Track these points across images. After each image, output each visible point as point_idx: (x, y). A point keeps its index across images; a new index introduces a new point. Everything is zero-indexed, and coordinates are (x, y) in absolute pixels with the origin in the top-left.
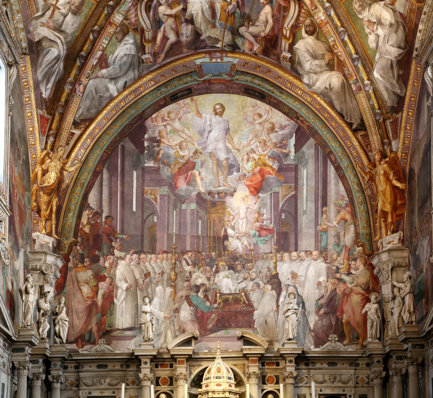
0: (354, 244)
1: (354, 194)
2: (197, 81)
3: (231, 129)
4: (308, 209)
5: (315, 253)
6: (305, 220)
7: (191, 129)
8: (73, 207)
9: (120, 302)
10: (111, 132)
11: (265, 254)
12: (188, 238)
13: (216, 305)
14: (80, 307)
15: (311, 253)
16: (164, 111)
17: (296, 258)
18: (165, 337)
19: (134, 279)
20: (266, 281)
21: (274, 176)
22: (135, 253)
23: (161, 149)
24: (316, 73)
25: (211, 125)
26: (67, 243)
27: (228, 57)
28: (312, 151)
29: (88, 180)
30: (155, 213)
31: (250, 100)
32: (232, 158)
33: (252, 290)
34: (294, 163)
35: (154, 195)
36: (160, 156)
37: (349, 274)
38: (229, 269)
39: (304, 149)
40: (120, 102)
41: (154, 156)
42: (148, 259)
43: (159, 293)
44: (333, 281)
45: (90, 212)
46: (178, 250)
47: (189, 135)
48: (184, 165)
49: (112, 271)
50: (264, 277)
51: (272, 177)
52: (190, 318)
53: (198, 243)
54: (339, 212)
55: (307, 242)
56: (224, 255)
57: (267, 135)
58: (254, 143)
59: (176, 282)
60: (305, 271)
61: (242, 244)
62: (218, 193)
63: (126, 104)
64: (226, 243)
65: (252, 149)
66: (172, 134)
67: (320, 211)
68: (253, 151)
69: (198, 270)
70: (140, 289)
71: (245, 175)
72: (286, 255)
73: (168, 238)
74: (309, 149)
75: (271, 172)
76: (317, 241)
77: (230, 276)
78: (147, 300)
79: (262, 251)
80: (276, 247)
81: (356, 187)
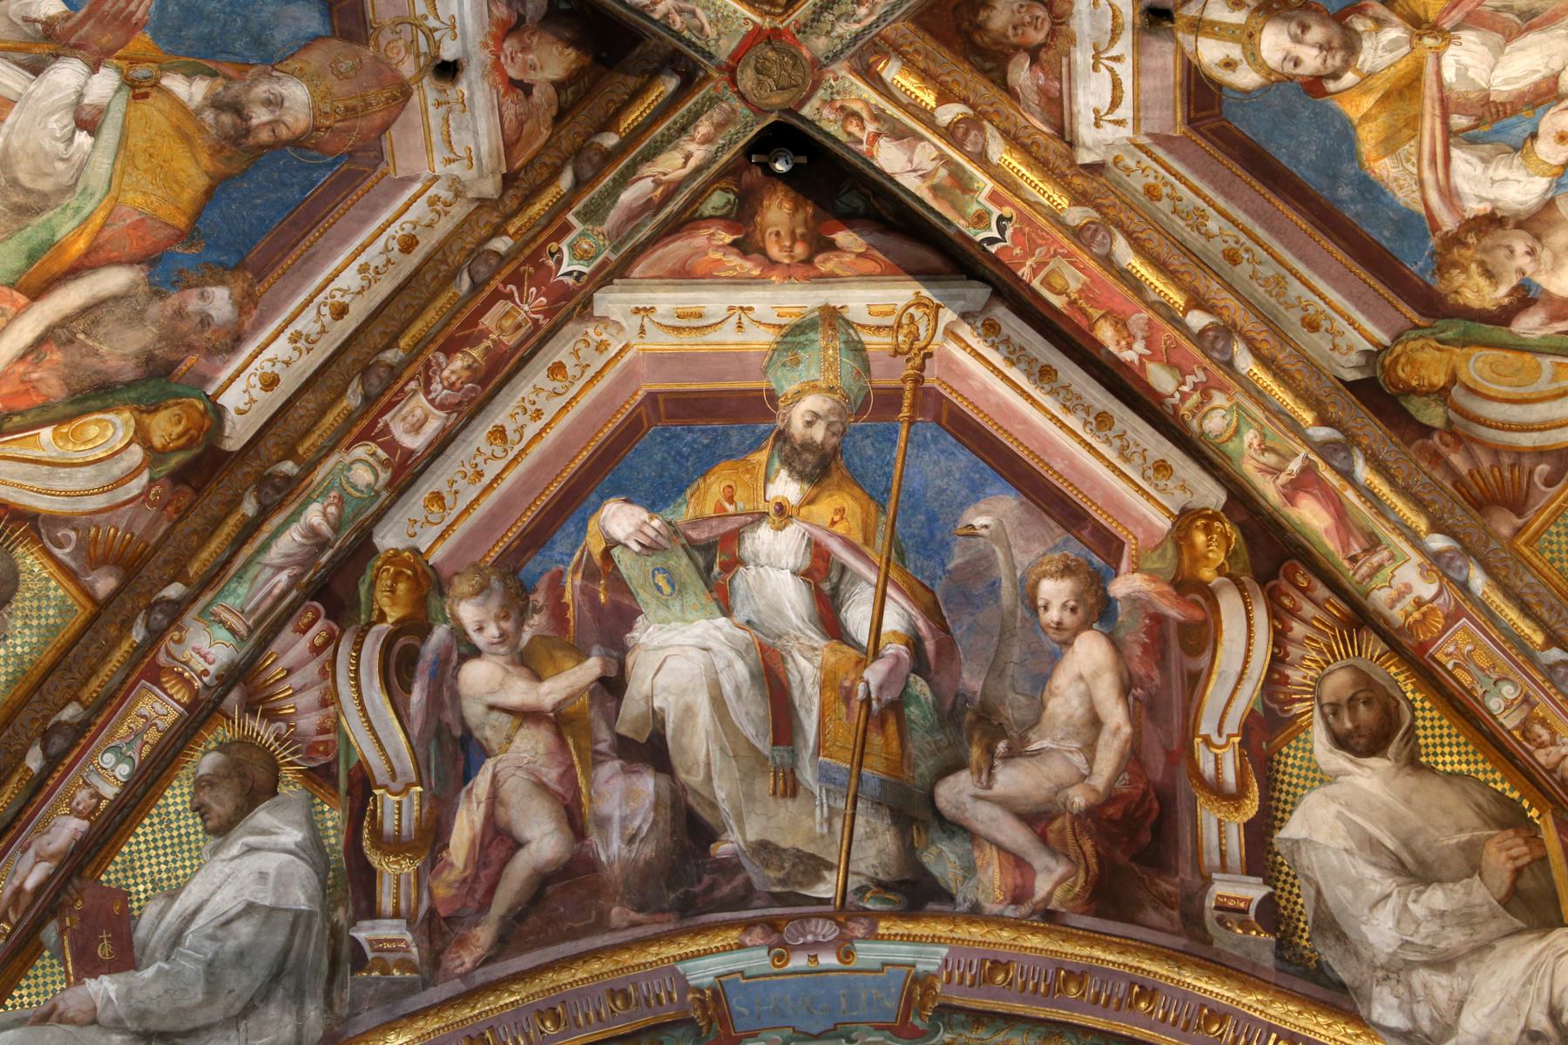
24: (1444, 963)
27: (882, 938)
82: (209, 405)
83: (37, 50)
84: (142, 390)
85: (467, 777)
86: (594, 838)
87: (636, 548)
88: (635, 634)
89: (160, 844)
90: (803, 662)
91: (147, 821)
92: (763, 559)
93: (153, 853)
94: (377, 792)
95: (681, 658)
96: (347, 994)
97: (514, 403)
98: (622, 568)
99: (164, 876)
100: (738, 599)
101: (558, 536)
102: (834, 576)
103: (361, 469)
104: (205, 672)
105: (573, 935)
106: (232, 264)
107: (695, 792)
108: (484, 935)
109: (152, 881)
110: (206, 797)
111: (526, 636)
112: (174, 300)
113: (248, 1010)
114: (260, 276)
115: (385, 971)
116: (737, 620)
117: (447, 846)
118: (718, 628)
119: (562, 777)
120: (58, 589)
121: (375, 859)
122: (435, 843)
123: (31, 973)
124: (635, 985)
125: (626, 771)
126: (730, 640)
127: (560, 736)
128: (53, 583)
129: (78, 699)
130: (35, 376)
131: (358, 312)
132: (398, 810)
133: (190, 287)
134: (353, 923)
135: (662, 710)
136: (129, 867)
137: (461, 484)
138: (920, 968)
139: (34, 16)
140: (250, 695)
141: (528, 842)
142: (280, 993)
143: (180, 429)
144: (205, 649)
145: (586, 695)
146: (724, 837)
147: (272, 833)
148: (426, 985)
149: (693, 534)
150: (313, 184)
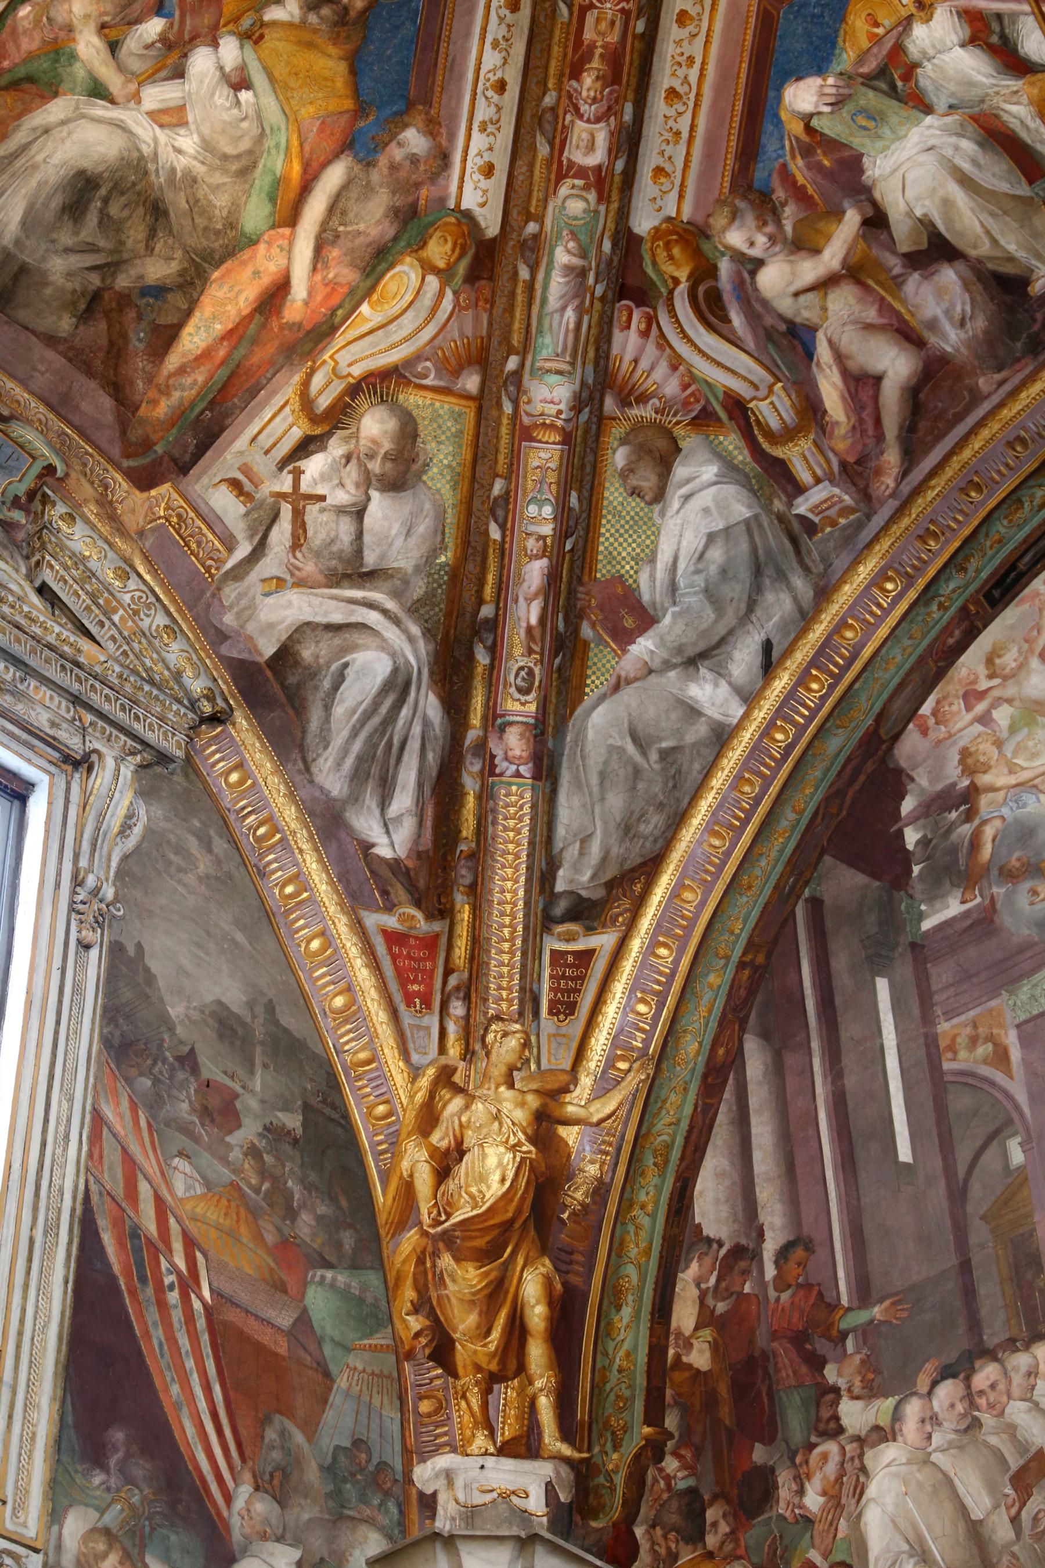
10: (758, 872)
16: (970, 662)
19: (961, 1527)
22: (947, 1373)
23: (984, 822)
30: (1009, 1122)
35: (990, 1038)
40: (768, 730)
41: (956, 868)
45: (708, 1260)
63: (802, 729)
66: (1025, 731)
82: (458, 215)
83: (170, 61)
84: (406, 236)
85: (809, 355)
86: (933, 340)
87: (827, 109)
88: (869, 173)
89: (622, 531)
90: (1013, 108)
91: (604, 521)
92: (931, 52)
93: (621, 540)
94: (750, 405)
95: (914, 168)
96: (815, 555)
97: (668, 64)
98: (826, 131)
99: (638, 550)
100: (932, 95)
101: (764, 140)
102: (995, 26)
103: (572, 203)
104: (560, 412)
105: (959, 418)
106: (403, 108)
107: (991, 259)
108: (892, 457)
109: (633, 559)
110: (633, 481)
111: (788, 228)
112: (383, 161)
113: (751, 606)
114: (428, 103)
115: (833, 523)
116: (940, 111)
117: (825, 412)
118: (929, 127)
119: (880, 312)
120: (444, 406)
121: (778, 452)
122: (815, 413)
123: (590, 663)
124: (1024, 428)
125: (926, 278)
126: (944, 129)
127: (859, 282)
128: (437, 404)
129: (497, 476)
130: (331, 276)
131: (513, 78)
132: (774, 409)
133: (387, 144)
134: (790, 505)
135: (925, 215)
136: (611, 558)
137: (669, 150)
139: (150, 41)
140: (619, 394)
141: (885, 372)
142: (767, 582)
143: (449, 245)
144: (549, 397)
145: (861, 240)
146: (1034, 277)
147: (695, 478)
148: (869, 517)
149: (865, 70)
150: (416, 12)
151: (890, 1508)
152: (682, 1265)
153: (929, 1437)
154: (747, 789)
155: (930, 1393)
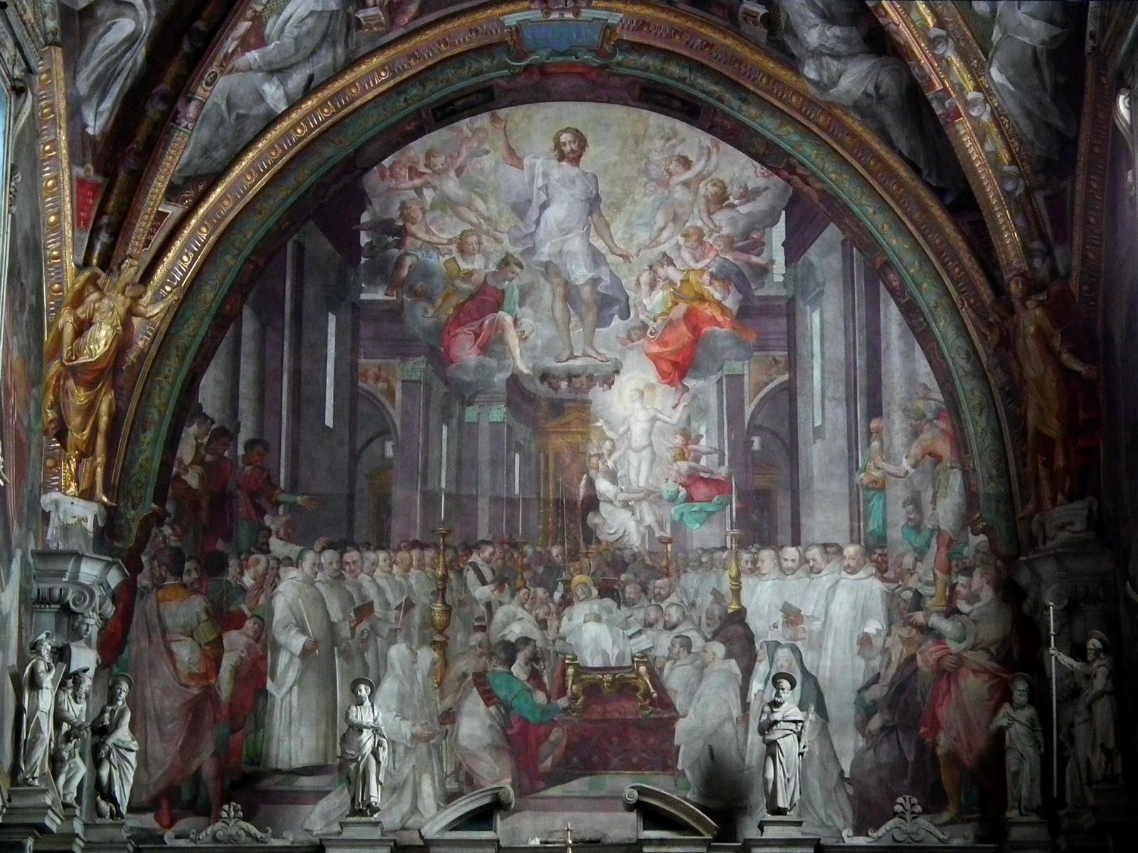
0: (963, 527)
1: (957, 382)
2: (508, 67)
3: (604, 198)
4: (828, 425)
5: (851, 550)
6: (820, 457)
7: (491, 199)
8: (155, 415)
9: (284, 690)
11: (705, 551)
12: (483, 504)
13: (563, 703)
14: (167, 703)
15: (840, 550)
16: (417, 149)
17: (794, 565)
18: (416, 796)
20: (708, 633)
21: (726, 329)
23: (407, 254)
25: (546, 187)
26: (134, 516)
27: (593, 8)
28: (835, 262)
29: (198, 340)
30: (388, 432)
31: (656, 120)
32: (607, 280)
33: (669, 659)
34: (783, 292)
35: (387, 380)
36: (405, 272)
37: (951, 611)
38: (602, 595)
39: (813, 254)
41: (385, 272)
42: (367, 564)
43: (397, 664)
44: (905, 632)
46: (454, 540)
47: (487, 214)
48: (472, 296)
49: (262, 600)
50: (704, 620)
51: (721, 332)
52: (488, 739)
53: (511, 521)
54: (916, 433)
55: (826, 517)
56: (587, 555)
57: (704, 215)
58: (669, 238)
59: (448, 632)
60: (822, 602)
61: (639, 522)
62: (570, 376)
64: (592, 519)
65: (665, 254)
67: (861, 429)
68: (668, 260)
69: (513, 596)
70: (343, 657)
71: (645, 326)
72: (767, 555)
73: (424, 505)
74: (826, 254)
75: (720, 318)
76: (857, 515)
77: (604, 617)
78: (364, 691)
79: (696, 544)
80: (736, 532)
81: (962, 362)
113: (313, 53)
115: (370, 28)
134: (356, 11)
138: (610, 21)
142: (326, 44)
151: (289, 599)
152: (188, 423)
153: (316, 574)
154: (273, 153)
155: (321, 552)
